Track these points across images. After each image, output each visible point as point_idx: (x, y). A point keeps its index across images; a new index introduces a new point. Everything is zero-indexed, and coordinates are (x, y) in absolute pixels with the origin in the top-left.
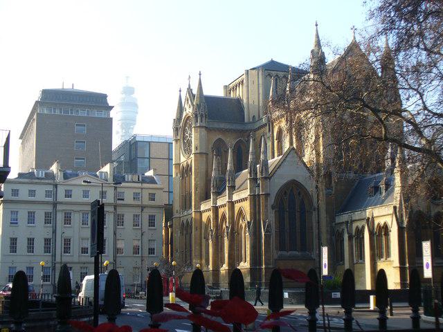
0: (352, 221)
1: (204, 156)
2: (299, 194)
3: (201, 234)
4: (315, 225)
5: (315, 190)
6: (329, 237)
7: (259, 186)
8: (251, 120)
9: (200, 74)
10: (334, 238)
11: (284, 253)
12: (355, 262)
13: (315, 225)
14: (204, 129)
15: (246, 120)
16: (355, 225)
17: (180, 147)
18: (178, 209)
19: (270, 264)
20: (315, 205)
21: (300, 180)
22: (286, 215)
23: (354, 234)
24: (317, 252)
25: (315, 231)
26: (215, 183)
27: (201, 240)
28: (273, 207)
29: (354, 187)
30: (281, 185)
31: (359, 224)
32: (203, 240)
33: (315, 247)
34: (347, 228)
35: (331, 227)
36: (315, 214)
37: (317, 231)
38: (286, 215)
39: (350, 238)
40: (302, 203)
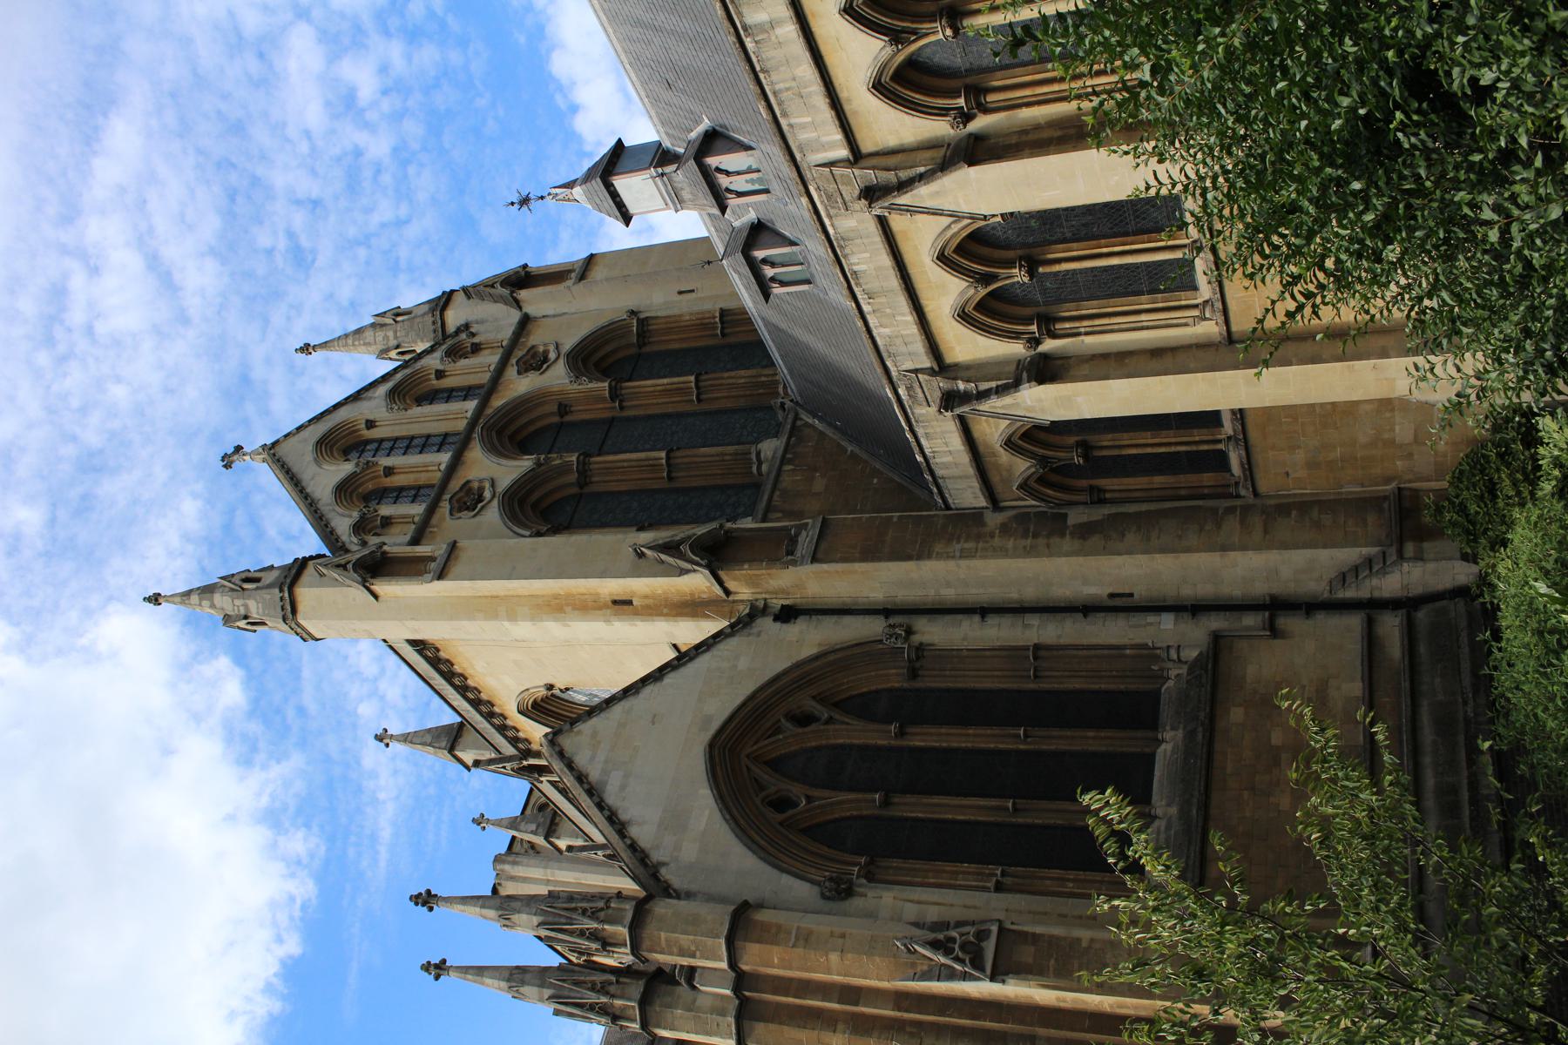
0: (942, 366)
2: (804, 720)
4: (997, 633)
6: (1067, 543)
7: (692, 971)
10: (1076, 516)
12: (1210, 328)
13: (997, 633)
16: (968, 346)
20: (873, 627)
21: (721, 707)
22: (913, 807)
23: (1017, 349)
24: (1167, 621)
28: (840, 891)
29: (829, 432)
30: (717, 815)
31: (946, 292)
34: (983, 395)
35: (1005, 529)
36: (932, 632)
37: (1034, 620)
38: (913, 807)
39: (1045, 370)
40: (862, 707)
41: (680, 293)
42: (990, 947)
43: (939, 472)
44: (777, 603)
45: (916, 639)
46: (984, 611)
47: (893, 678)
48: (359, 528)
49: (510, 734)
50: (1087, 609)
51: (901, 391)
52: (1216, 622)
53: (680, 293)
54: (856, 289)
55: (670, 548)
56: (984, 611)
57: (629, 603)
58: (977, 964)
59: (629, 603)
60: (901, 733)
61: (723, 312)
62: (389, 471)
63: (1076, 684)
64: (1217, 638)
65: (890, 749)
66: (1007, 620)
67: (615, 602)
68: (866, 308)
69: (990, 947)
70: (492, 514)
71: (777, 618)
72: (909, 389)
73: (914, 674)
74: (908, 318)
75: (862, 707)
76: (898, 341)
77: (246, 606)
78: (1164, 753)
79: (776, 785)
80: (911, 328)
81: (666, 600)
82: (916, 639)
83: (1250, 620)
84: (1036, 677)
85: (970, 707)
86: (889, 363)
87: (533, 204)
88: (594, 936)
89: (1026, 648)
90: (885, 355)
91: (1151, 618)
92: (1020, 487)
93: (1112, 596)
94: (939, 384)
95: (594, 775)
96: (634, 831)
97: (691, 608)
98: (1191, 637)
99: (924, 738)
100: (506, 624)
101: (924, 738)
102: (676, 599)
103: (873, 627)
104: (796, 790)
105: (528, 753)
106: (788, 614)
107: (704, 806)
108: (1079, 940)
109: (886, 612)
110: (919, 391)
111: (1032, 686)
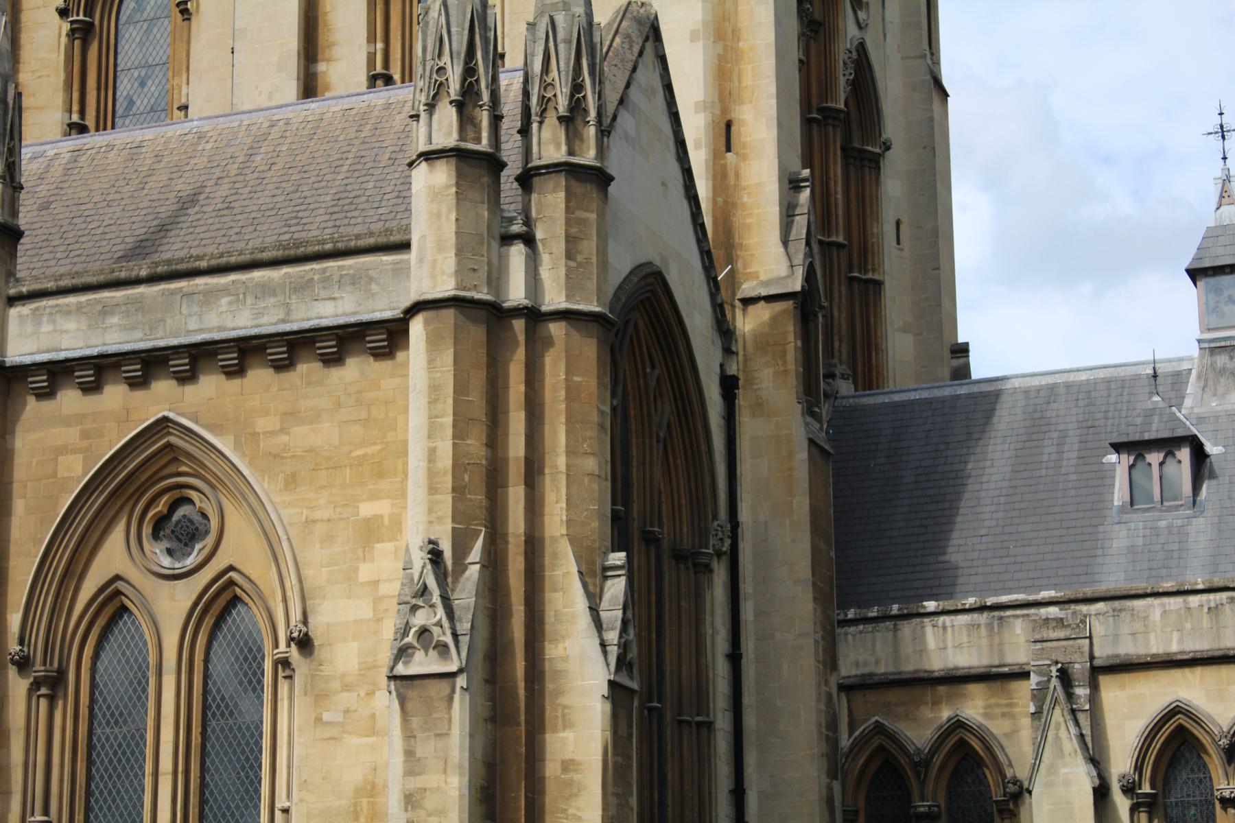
41: (898, 223)
43: (907, 628)
46: (735, 658)
51: (1053, 611)
53: (898, 223)
54: (1224, 595)
56: (735, 658)
57: (728, 149)
59: (728, 149)
61: (878, 284)
67: (729, 125)
68: (1194, 600)
72: (1060, 622)
74: (1174, 646)
76: (1138, 626)
80: (1155, 646)
81: (734, 205)
84: (680, 723)
86: (1101, 606)
87: (1215, 140)
88: (577, 106)
90: (1117, 604)
92: (879, 729)
94: (1079, 668)
102: (737, 220)
110: (1061, 634)
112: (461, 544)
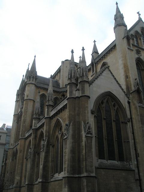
1: (32, 101)
2: (114, 106)
3: (23, 156)
4: (130, 135)
5: (127, 104)
8: (64, 86)
9: (35, 57)
11: (104, 161)
13: (130, 135)
14: (34, 86)
15: (61, 86)
17: (19, 106)
18: (13, 143)
19: (92, 172)
20: (129, 117)
21: (114, 93)
22: (104, 123)
24: (136, 163)
25: (131, 142)
26: (37, 112)
27: (23, 160)
28: (92, 112)
30: (100, 93)
32: (25, 160)
33: (132, 156)
36: (129, 124)
37: (133, 141)
38: (104, 123)
42: (89, 135)
44: (130, 101)
45: (128, 123)
47: (122, 120)
48: (132, 35)
49: (99, 61)
50: (136, 150)
52: (136, 171)
55: (138, 84)
58: (88, 133)
60: (114, 121)
62: (140, 39)
63: (124, 148)
64: (134, 171)
65: (111, 119)
66: (132, 137)
69: (89, 135)
70: (137, 56)
71: (128, 101)
73: (122, 123)
75: (117, 115)
77: (118, 18)
78: (115, 162)
79: (105, 101)
82: (128, 123)
83: (137, 176)
84: (124, 142)
85: (119, 131)
89: (129, 140)
91: (135, 160)
93: (138, 154)
95: (103, 74)
96: (96, 80)
97: (128, 88)
98: (133, 167)
99: (114, 124)
100: (121, 59)
101: (114, 124)
103: (129, 117)
104: (104, 105)
105: (96, 64)
106: (129, 103)
107: (101, 91)
108: (92, 149)
109: (131, 118)
111: (123, 141)
112: (70, 123)
